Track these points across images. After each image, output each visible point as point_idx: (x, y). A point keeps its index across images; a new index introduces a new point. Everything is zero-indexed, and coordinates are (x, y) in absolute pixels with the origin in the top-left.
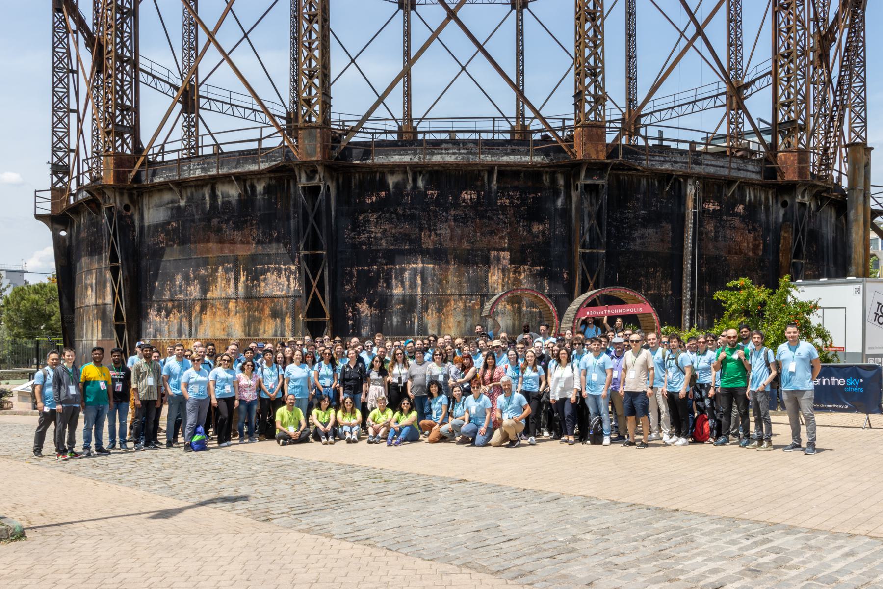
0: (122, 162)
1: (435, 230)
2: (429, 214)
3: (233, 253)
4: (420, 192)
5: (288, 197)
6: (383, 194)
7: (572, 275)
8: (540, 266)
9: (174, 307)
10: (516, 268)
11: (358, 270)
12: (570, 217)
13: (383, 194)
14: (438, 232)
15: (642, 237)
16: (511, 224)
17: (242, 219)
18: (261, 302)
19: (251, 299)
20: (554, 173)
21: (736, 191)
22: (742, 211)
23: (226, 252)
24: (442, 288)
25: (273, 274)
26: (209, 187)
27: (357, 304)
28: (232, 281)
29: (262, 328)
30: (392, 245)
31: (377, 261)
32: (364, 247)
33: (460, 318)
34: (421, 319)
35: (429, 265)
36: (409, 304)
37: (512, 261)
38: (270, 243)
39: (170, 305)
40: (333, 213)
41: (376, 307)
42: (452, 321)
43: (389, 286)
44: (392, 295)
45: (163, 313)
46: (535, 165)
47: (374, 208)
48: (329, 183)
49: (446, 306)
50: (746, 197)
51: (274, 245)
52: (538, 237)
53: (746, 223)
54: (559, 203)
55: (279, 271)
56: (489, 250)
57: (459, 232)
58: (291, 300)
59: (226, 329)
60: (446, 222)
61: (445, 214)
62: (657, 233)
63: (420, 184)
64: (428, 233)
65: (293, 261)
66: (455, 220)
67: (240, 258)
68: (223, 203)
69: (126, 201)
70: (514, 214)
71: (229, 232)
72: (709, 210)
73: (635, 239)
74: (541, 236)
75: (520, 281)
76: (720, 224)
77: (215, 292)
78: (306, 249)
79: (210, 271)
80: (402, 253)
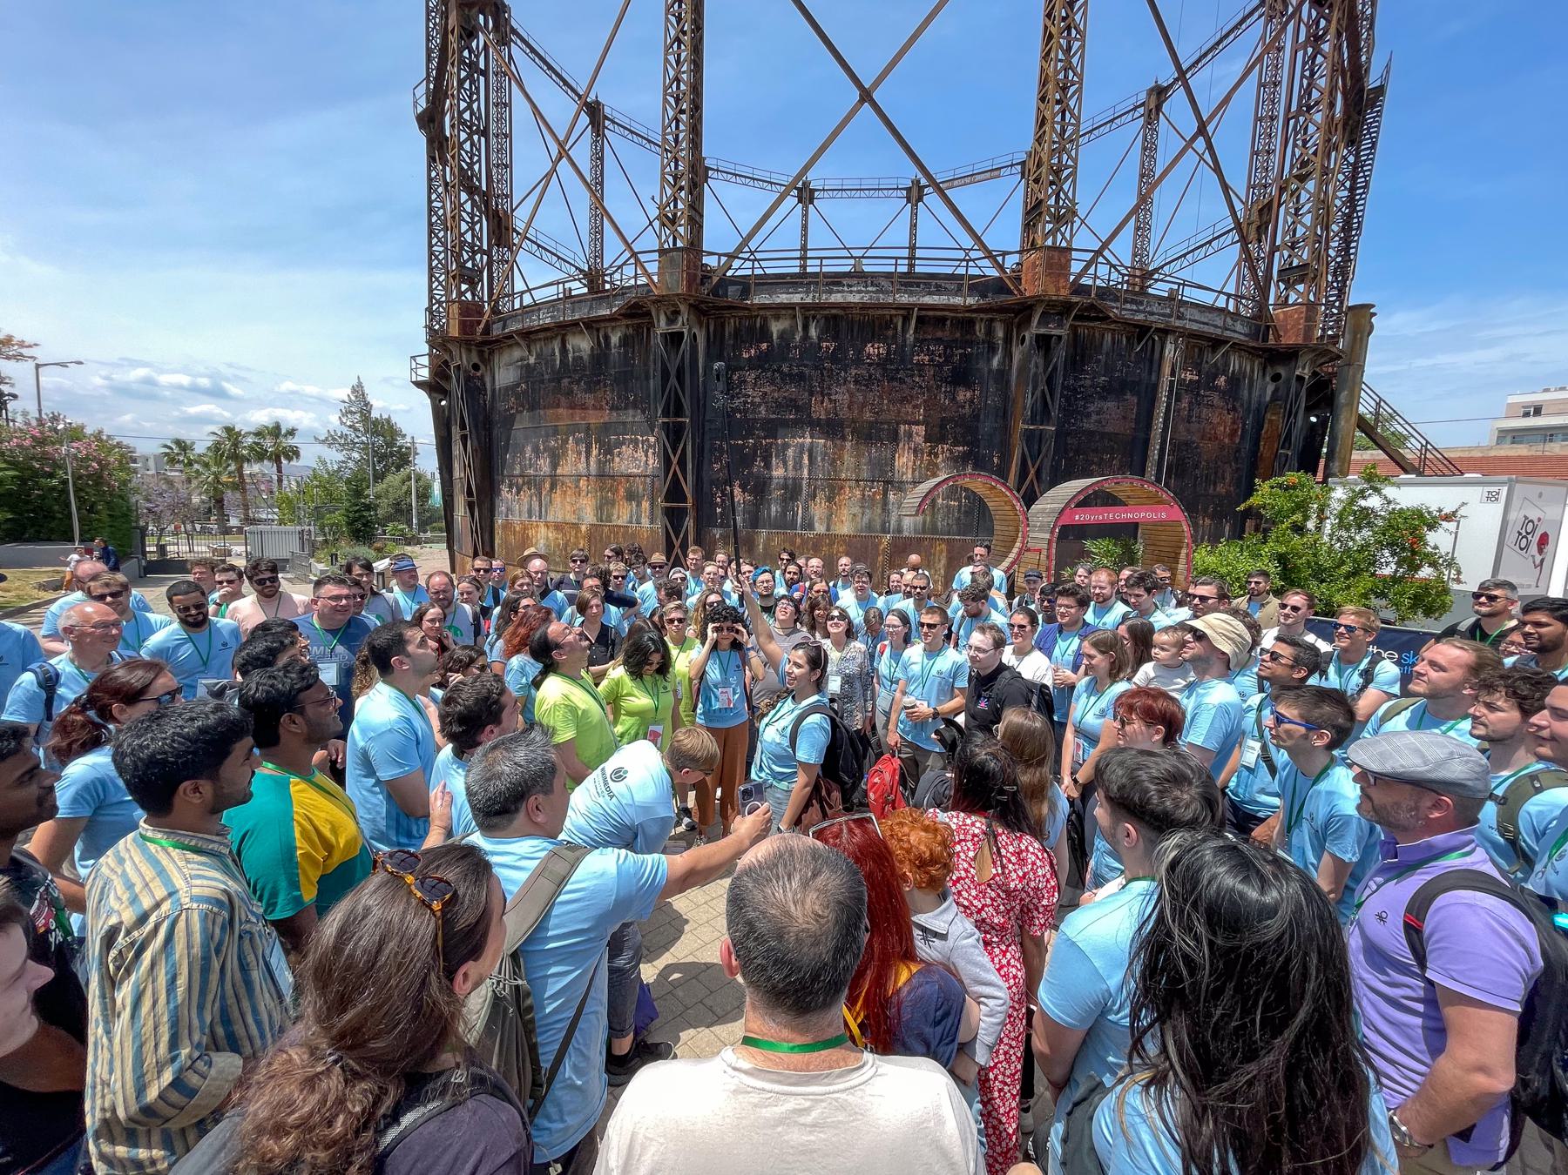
0: (470, 311)
1: (830, 394)
2: (822, 374)
5: (647, 351)
7: (1006, 457)
9: (524, 483)
12: (1008, 382)
13: (764, 346)
16: (929, 389)
19: (604, 476)
20: (992, 320)
23: (577, 420)
24: (835, 471)
26: (559, 338)
28: (584, 454)
29: (615, 512)
32: (738, 416)
33: (856, 510)
34: (806, 509)
36: (792, 491)
38: (626, 409)
39: (520, 481)
41: (750, 494)
42: (845, 514)
43: (768, 466)
44: (771, 478)
45: (514, 490)
46: (969, 309)
47: (753, 364)
48: (695, 330)
49: (839, 494)
51: (631, 412)
54: (995, 362)
55: (636, 442)
56: (898, 424)
58: (648, 480)
61: (843, 374)
63: (813, 333)
65: (652, 431)
66: (856, 382)
67: (592, 426)
69: (476, 360)
71: (581, 395)
75: (936, 465)
78: (666, 413)
80: (785, 424)
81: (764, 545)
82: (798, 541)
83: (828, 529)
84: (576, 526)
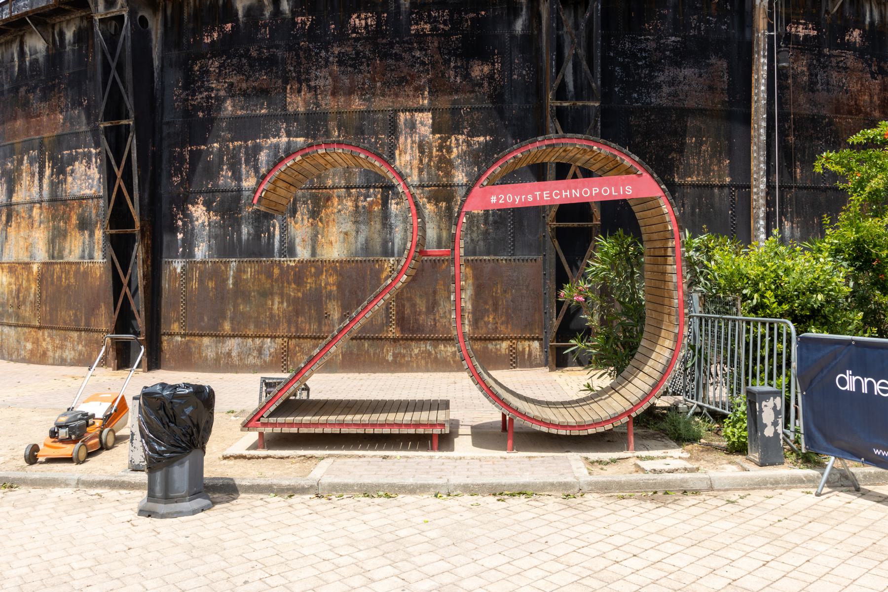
1: (308, 80)
2: (298, 55)
3: (39, 135)
4: (285, 19)
6: (229, 26)
8: (485, 136)
10: (444, 140)
11: (191, 151)
12: (539, 50)
13: (229, 25)
14: (312, 84)
15: (672, 83)
16: (434, 64)
17: (50, 83)
18: (67, 206)
21: (847, 6)
22: (858, 40)
23: (33, 135)
25: (81, 163)
27: (190, 206)
28: (37, 175)
30: (242, 108)
31: (220, 136)
32: (201, 114)
33: (349, 226)
35: (299, 139)
37: (436, 129)
40: (156, 63)
41: (216, 212)
44: (240, 190)
47: (216, 50)
49: (325, 207)
50: (864, 16)
52: (481, 85)
53: (866, 61)
54: (519, 26)
55: (88, 156)
56: (396, 111)
57: (347, 82)
59: (29, 249)
60: (326, 66)
61: (323, 54)
62: (700, 76)
64: (296, 86)
66: (341, 63)
67: (46, 141)
68: (30, 63)
70: (439, 48)
71: (36, 104)
72: (797, 37)
73: (660, 87)
74: (486, 84)
75: (450, 162)
76: (818, 61)
77: (20, 193)
79: (15, 163)
81: (234, 277)
82: (276, 271)
83: (314, 253)
84: (27, 265)
